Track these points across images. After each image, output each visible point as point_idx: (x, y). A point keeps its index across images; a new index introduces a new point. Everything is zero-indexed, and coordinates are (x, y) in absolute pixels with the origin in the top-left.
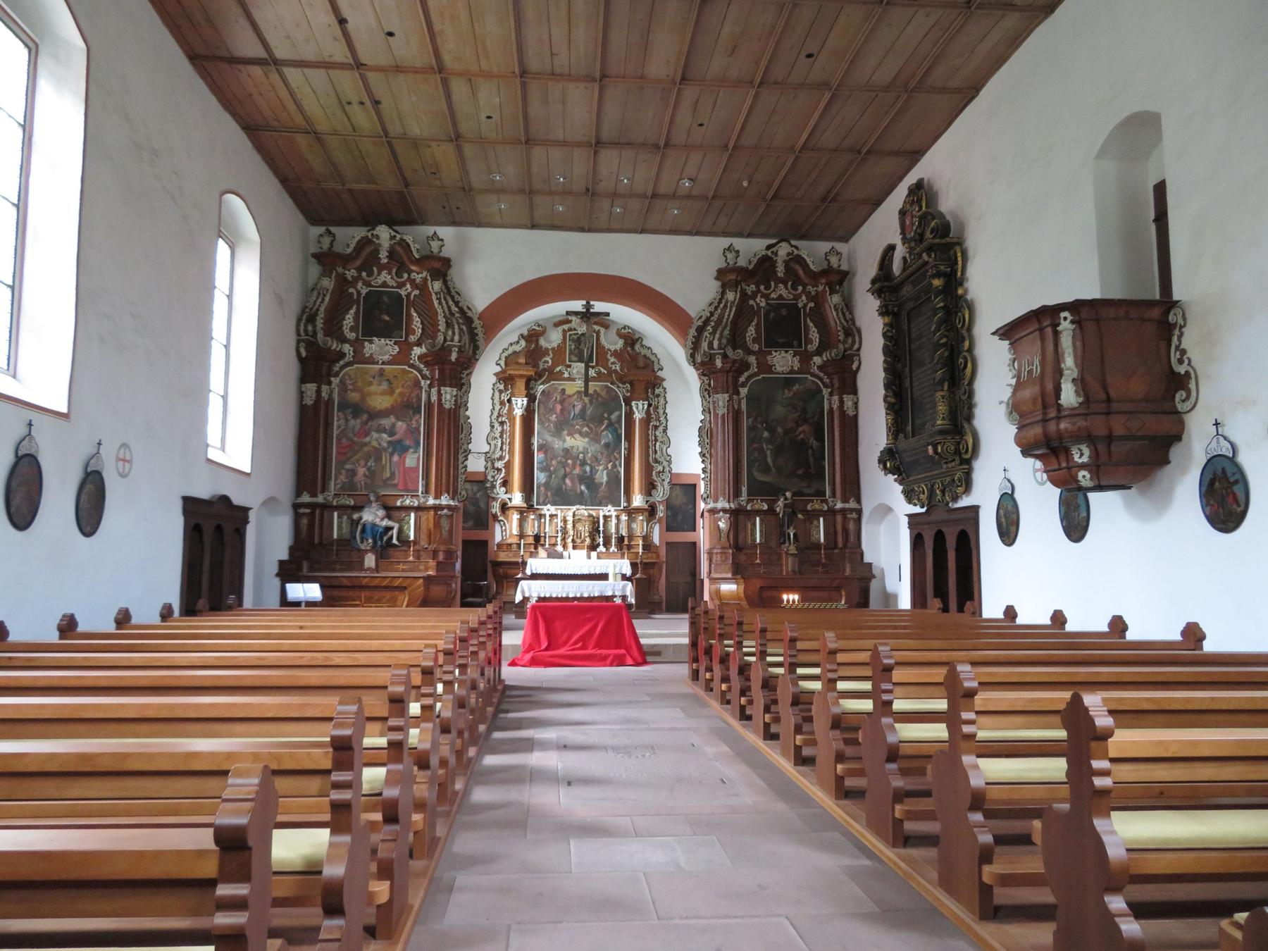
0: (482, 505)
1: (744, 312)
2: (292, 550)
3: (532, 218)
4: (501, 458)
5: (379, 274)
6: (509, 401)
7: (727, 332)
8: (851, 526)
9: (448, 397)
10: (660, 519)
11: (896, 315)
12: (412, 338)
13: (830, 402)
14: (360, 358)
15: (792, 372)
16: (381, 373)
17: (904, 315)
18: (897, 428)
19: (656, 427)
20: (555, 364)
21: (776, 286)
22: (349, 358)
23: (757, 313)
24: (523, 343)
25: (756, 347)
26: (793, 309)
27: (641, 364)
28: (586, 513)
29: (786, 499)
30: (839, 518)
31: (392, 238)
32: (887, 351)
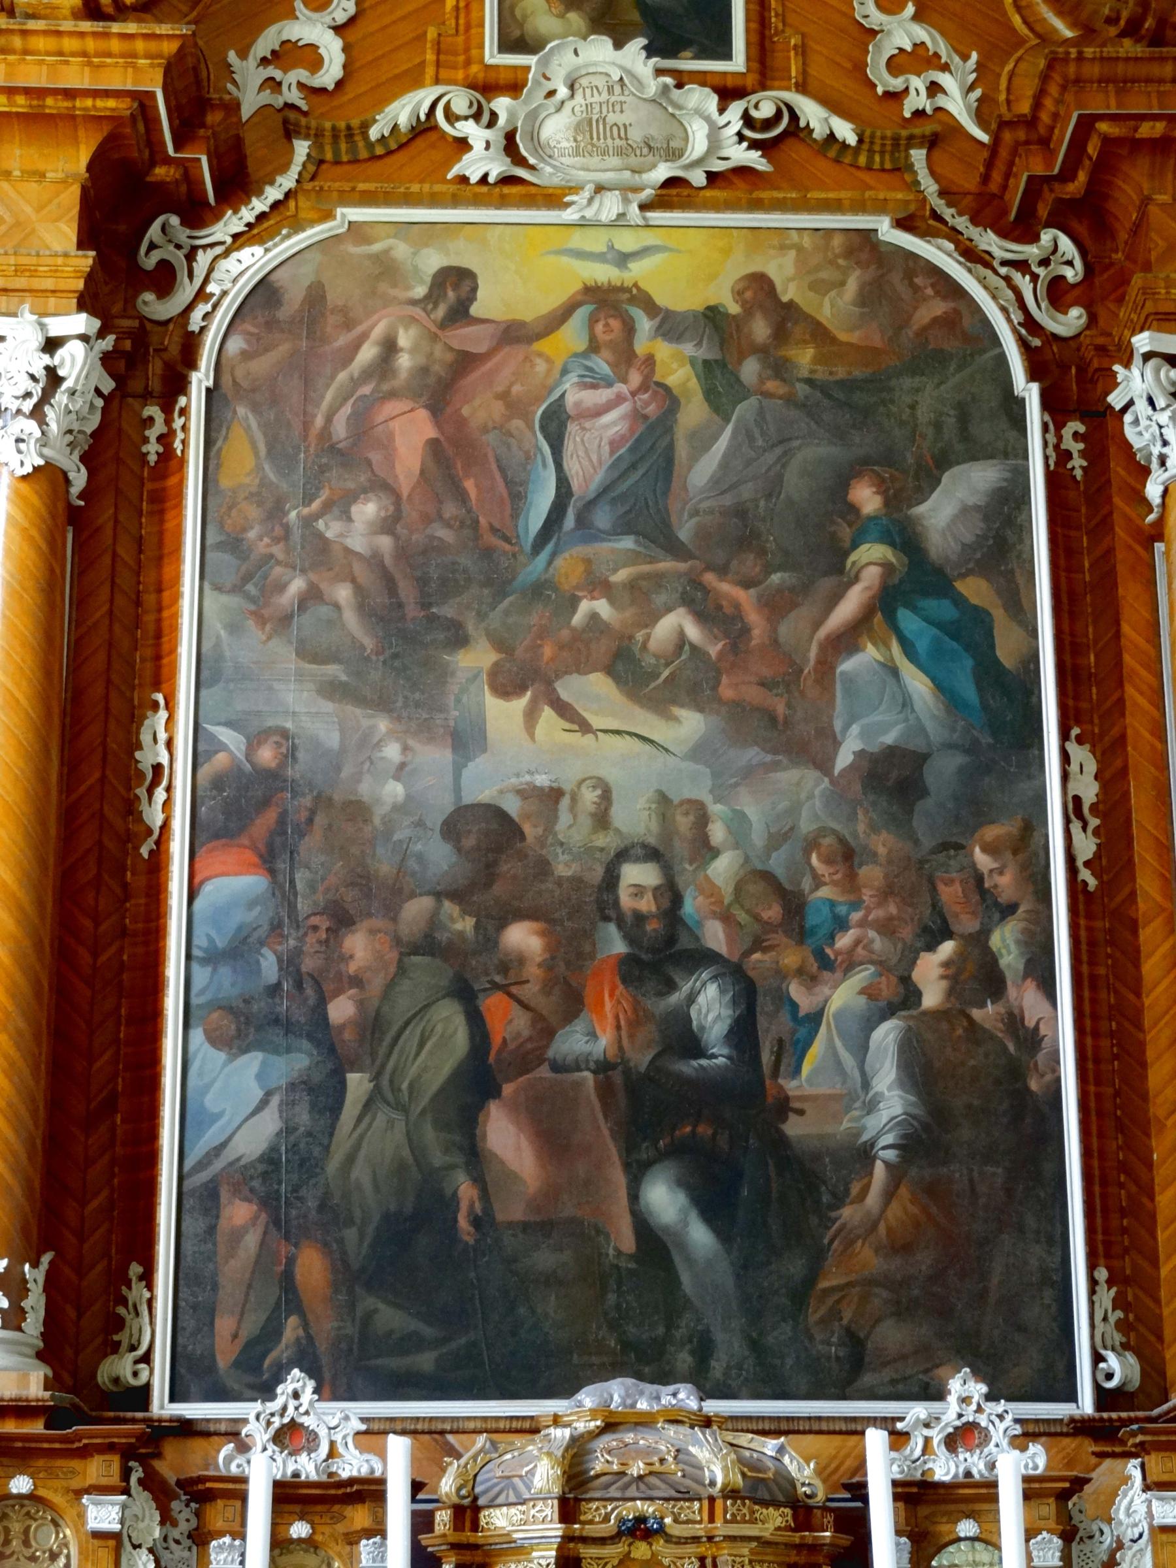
28: (714, 1464)
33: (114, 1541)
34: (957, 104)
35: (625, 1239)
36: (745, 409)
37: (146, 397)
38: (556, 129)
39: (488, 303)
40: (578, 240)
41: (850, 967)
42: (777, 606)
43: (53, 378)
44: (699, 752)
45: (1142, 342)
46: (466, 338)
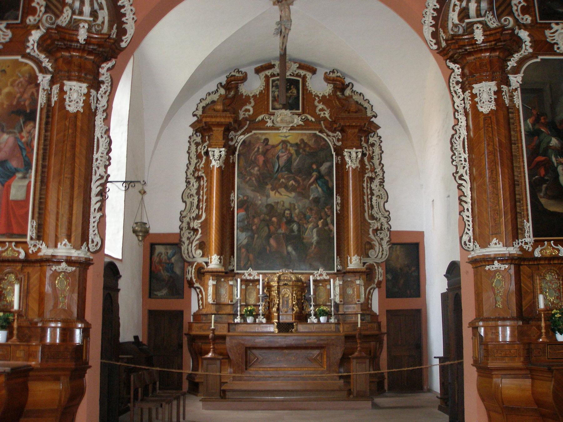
0: (178, 271)
4: (198, 217)
6: (207, 153)
10: (379, 283)
19: (372, 179)
20: (257, 113)
24: (222, 91)
27: (353, 108)
33: (232, 285)
34: (327, 115)
35: (285, 253)
36: (300, 156)
37: (230, 155)
39: (270, 143)
40: (281, 135)
41: (311, 222)
42: (304, 180)
43: (221, 155)
44: (294, 197)
45: (346, 150)
46: (268, 147)
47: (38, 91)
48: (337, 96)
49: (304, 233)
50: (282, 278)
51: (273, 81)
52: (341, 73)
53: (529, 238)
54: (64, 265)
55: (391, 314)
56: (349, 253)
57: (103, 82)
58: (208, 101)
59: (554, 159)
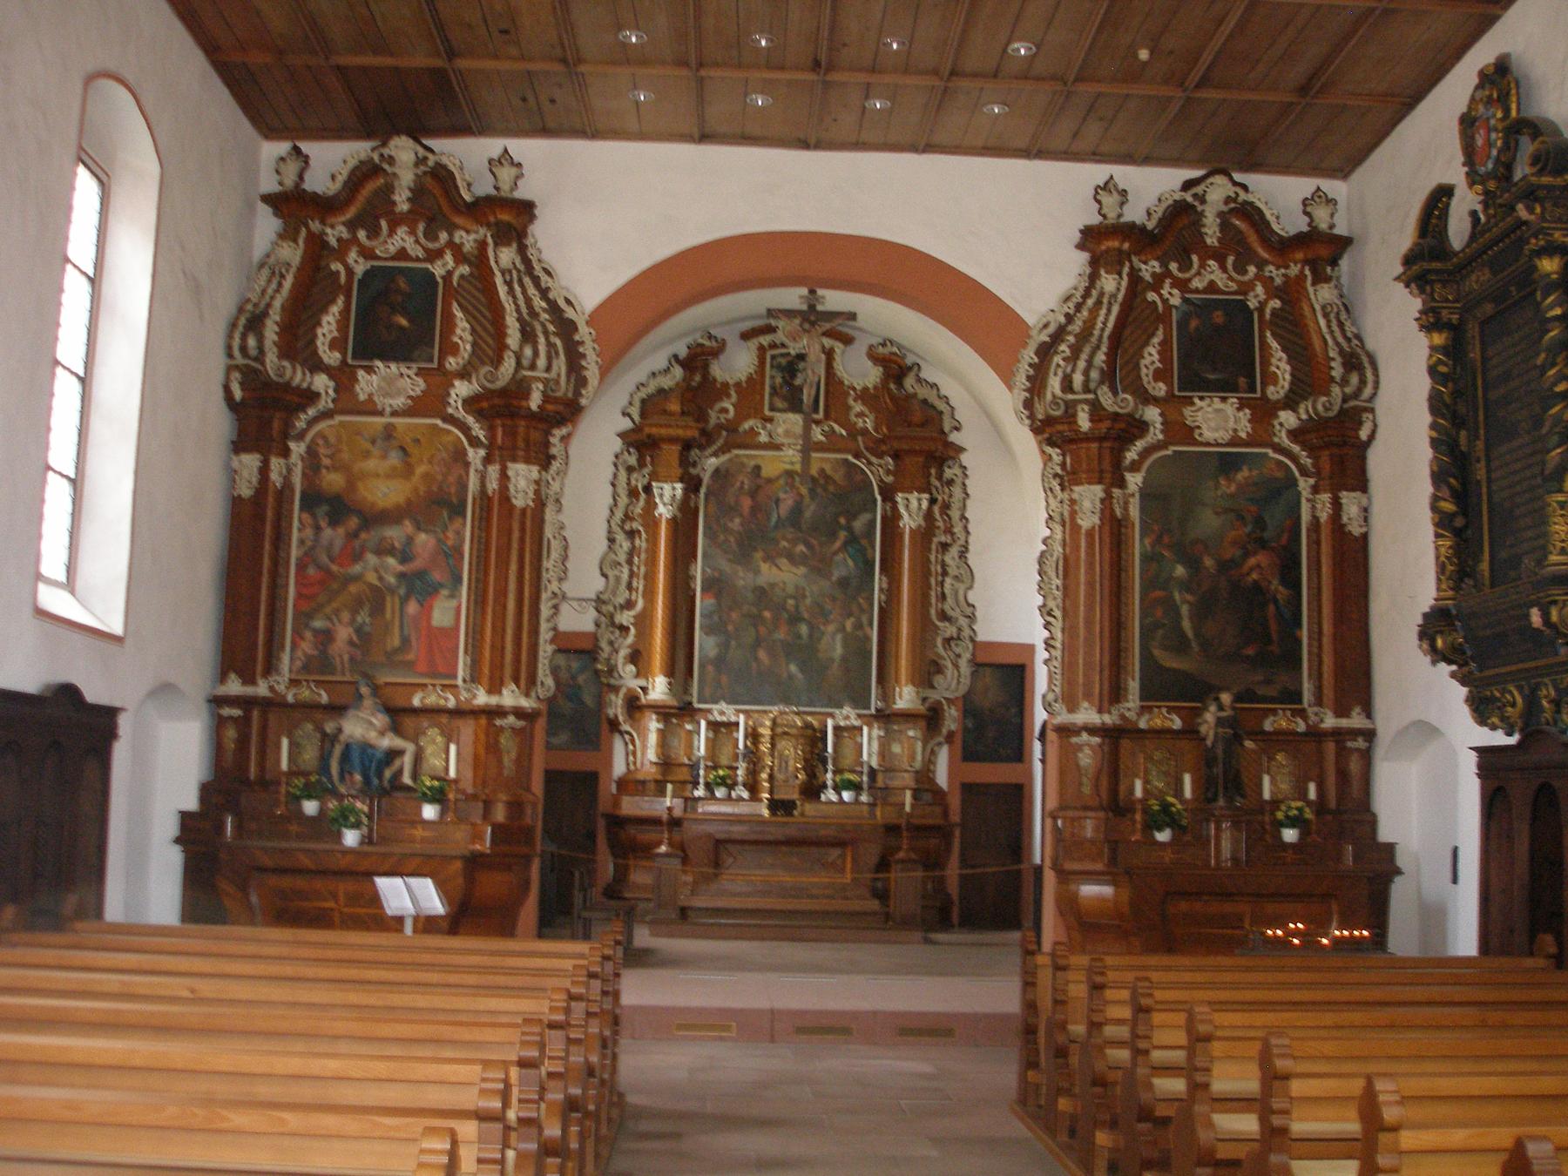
0: (589, 700)
1: (1135, 316)
2: (206, 791)
3: (701, 118)
4: (629, 605)
5: (392, 232)
6: (648, 489)
7: (1100, 357)
8: (1354, 766)
9: (522, 484)
11: (1456, 332)
12: (452, 363)
13: (1313, 505)
14: (346, 400)
15: (1235, 441)
16: (389, 432)
17: (1473, 330)
18: (1458, 567)
19: (945, 547)
21: (1203, 265)
22: (325, 403)
23: (1164, 318)
24: (678, 372)
25: (1160, 389)
26: (1238, 310)
27: (917, 417)
29: (1221, 708)
30: (1330, 747)
31: (421, 161)
32: (1436, 404)
38: (780, 430)
39: (765, 473)
47: (467, 474)
48: (889, 390)
49: (819, 640)
50: (779, 721)
51: (773, 357)
52: (900, 347)
53: (1133, 701)
54: (511, 719)
55: (968, 789)
56: (897, 681)
57: (554, 457)
58: (651, 389)
59: (1177, 596)
